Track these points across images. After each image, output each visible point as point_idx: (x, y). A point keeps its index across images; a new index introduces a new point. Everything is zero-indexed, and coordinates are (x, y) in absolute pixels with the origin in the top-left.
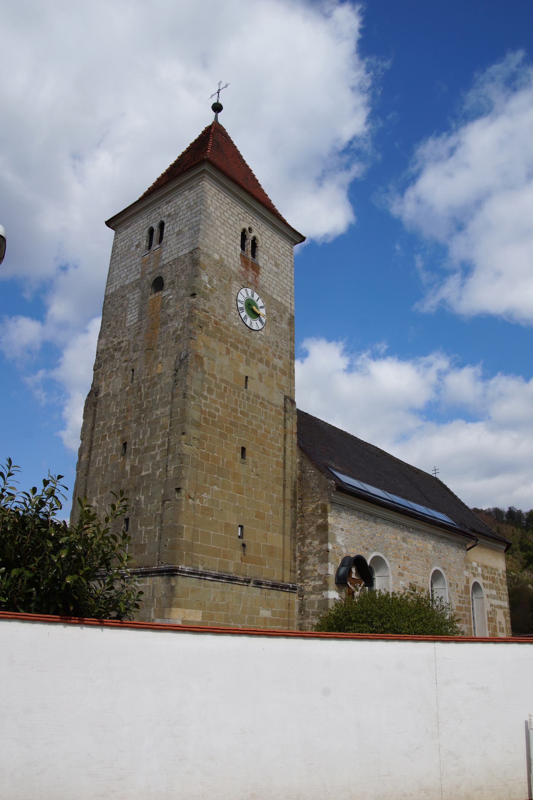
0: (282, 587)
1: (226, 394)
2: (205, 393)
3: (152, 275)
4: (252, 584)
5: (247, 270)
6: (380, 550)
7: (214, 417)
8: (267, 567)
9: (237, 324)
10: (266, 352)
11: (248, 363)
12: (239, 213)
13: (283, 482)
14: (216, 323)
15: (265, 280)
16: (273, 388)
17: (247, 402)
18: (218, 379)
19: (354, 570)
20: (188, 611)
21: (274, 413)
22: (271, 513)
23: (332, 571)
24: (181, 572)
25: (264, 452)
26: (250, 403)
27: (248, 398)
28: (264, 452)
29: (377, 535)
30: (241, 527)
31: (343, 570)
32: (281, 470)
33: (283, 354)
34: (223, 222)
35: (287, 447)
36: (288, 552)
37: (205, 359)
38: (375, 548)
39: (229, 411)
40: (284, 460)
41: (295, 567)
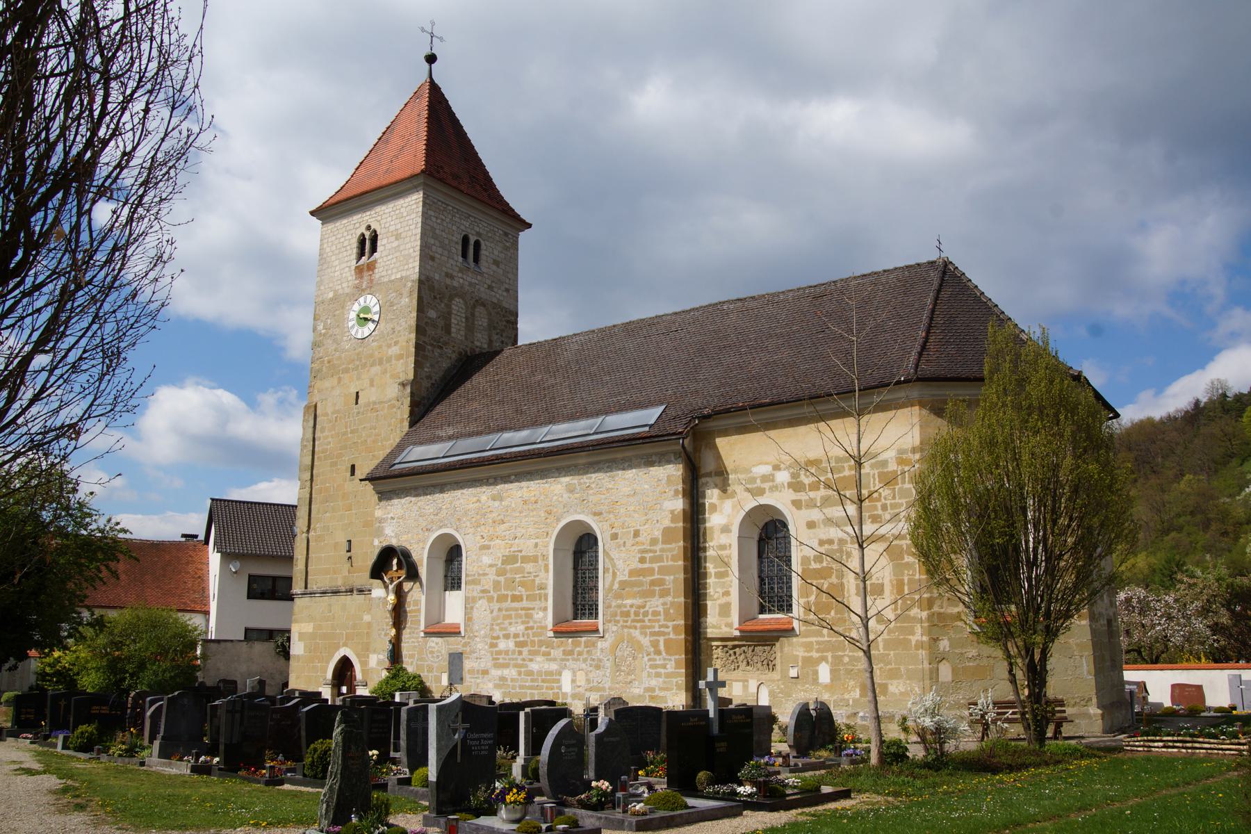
5: (362, 277)
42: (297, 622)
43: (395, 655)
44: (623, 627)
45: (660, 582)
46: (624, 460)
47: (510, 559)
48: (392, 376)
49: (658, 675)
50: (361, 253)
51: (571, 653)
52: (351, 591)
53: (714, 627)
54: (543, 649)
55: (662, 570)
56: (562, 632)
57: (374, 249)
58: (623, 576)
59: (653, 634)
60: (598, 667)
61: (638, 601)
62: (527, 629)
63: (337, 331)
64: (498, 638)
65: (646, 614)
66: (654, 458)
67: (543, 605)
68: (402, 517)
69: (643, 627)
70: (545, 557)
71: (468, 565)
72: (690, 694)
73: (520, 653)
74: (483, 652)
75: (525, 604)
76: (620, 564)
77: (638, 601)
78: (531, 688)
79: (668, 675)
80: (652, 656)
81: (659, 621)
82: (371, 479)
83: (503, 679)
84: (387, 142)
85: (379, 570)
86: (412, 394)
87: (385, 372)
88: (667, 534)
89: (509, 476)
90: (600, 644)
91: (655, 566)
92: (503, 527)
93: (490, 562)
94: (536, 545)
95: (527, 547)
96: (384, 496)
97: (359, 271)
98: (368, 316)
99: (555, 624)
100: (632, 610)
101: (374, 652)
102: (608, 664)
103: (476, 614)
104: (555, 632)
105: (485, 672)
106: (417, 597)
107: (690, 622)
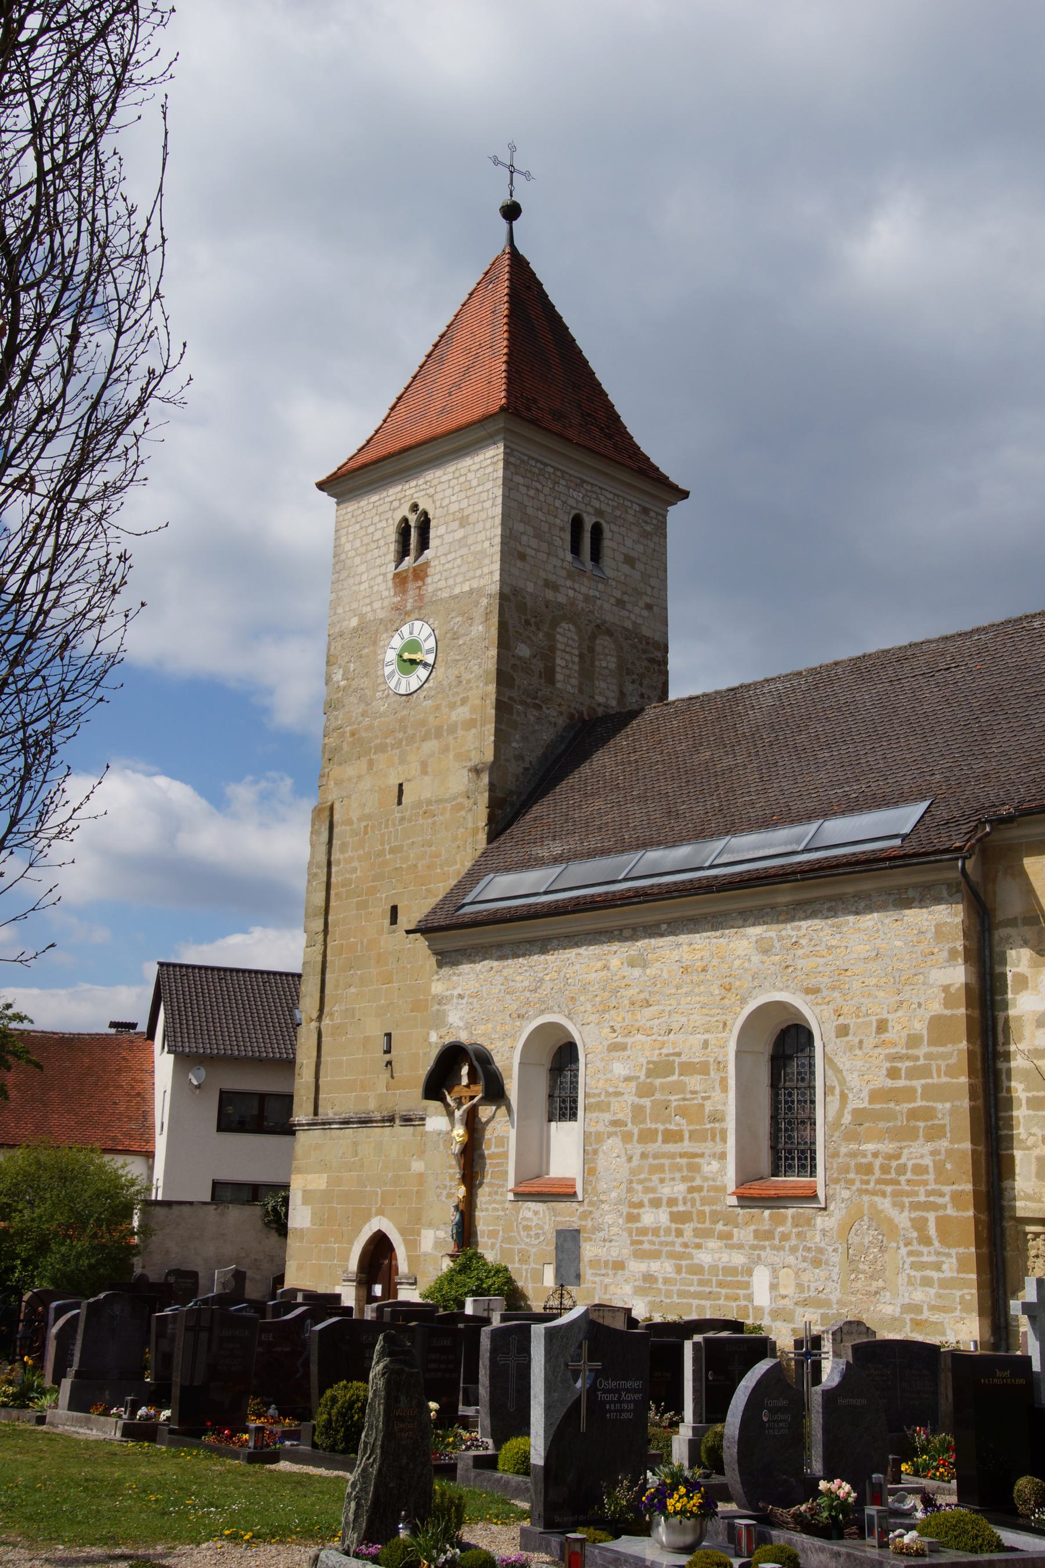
4: (397, 1121)
5: (404, 592)
6: (556, 1009)
12: (391, 502)
20: (310, 1177)
29: (547, 978)
30: (389, 1035)
38: (543, 1007)
42: (299, 1171)
43: (465, 1232)
44: (861, 1192)
45: (927, 1114)
46: (858, 896)
47: (660, 1068)
48: (458, 757)
49: (927, 1282)
50: (403, 551)
51: (769, 1235)
52: (391, 1119)
53: (1028, 1198)
54: (720, 1227)
55: (930, 1092)
56: (752, 1199)
57: (424, 544)
58: (859, 1101)
59: (915, 1206)
60: (817, 1263)
61: (888, 1147)
62: (691, 1190)
63: (365, 682)
64: (641, 1205)
65: (902, 1170)
66: (911, 893)
67: (719, 1149)
68: (476, 995)
69: (896, 1194)
70: (721, 1065)
71: (591, 1076)
72: (987, 1322)
73: (679, 1233)
74: (614, 1230)
75: (687, 1146)
76: (853, 1080)
77: (888, 1147)
78: (697, 1295)
79: (944, 1284)
80: (915, 1247)
81: (925, 1183)
82: (424, 929)
83: (649, 1278)
84: (441, 361)
85: (438, 1084)
86: (492, 787)
87: (446, 750)
88: (938, 1026)
89: (658, 925)
90: (821, 1221)
91: (918, 1084)
92: (649, 1012)
93: (625, 1072)
94: (706, 1044)
95: (689, 1046)
96: (446, 958)
97: (401, 580)
98: (418, 657)
99: (740, 1184)
100: (877, 1163)
101: (430, 1225)
102: (835, 1258)
103: (601, 1162)
104: (740, 1198)
105: (619, 1265)
106: (502, 1131)
107: (983, 1188)
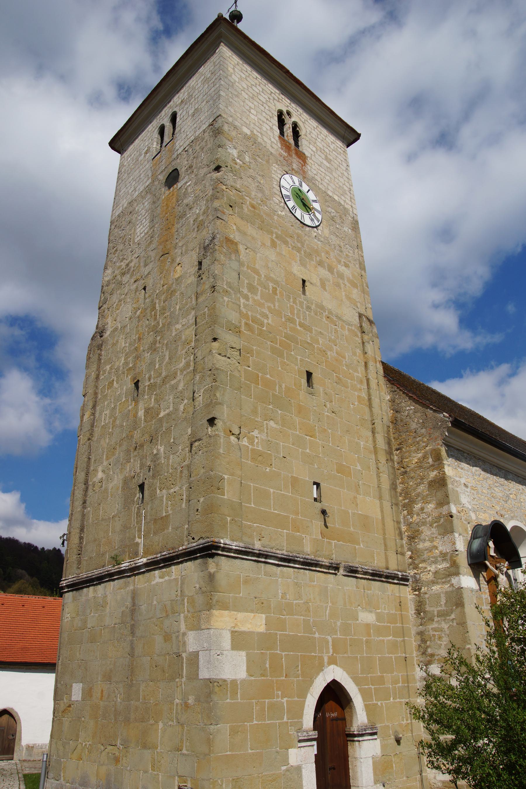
0: (387, 577)
1: (276, 297)
2: (245, 291)
3: (164, 173)
4: (341, 571)
7: (262, 325)
8: (362, 546)
9: (283, 213)
10: (327, 255)
11: (303, 264)
13: (371, 426)
14: (253, 207)
15: (315, 172)
16: (342, 300)
17: (307, 313)
18: (263, 276)
19: (491, 544)
20: (240, 615)
21: (347, 332)
22: (359, 468)
23: (461, 546)
24: (223, 549)
25: (339, 381)
26: (312, 314)
27: (309, 308)
28: (339, 381)
29: (511, 496)
30: (318, 485)
31: (476, 544)
32: (367, 409)
33: (350, 262)
34: (251, 95)
35: (370, 377)
36: (390, 525)
37: (241, 248)
38: (512, 515)
39: (283, 320)
40: (369, 395)
41: (402, 546)
42: (226, 607)
